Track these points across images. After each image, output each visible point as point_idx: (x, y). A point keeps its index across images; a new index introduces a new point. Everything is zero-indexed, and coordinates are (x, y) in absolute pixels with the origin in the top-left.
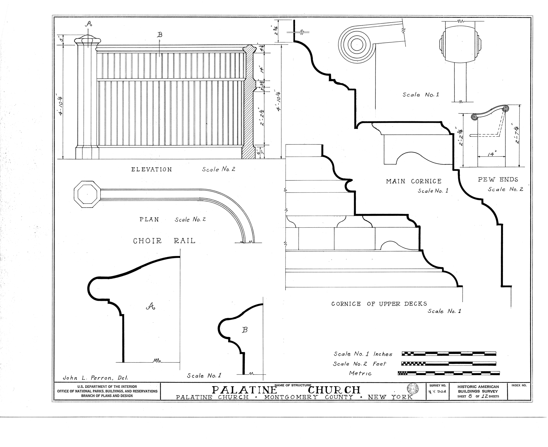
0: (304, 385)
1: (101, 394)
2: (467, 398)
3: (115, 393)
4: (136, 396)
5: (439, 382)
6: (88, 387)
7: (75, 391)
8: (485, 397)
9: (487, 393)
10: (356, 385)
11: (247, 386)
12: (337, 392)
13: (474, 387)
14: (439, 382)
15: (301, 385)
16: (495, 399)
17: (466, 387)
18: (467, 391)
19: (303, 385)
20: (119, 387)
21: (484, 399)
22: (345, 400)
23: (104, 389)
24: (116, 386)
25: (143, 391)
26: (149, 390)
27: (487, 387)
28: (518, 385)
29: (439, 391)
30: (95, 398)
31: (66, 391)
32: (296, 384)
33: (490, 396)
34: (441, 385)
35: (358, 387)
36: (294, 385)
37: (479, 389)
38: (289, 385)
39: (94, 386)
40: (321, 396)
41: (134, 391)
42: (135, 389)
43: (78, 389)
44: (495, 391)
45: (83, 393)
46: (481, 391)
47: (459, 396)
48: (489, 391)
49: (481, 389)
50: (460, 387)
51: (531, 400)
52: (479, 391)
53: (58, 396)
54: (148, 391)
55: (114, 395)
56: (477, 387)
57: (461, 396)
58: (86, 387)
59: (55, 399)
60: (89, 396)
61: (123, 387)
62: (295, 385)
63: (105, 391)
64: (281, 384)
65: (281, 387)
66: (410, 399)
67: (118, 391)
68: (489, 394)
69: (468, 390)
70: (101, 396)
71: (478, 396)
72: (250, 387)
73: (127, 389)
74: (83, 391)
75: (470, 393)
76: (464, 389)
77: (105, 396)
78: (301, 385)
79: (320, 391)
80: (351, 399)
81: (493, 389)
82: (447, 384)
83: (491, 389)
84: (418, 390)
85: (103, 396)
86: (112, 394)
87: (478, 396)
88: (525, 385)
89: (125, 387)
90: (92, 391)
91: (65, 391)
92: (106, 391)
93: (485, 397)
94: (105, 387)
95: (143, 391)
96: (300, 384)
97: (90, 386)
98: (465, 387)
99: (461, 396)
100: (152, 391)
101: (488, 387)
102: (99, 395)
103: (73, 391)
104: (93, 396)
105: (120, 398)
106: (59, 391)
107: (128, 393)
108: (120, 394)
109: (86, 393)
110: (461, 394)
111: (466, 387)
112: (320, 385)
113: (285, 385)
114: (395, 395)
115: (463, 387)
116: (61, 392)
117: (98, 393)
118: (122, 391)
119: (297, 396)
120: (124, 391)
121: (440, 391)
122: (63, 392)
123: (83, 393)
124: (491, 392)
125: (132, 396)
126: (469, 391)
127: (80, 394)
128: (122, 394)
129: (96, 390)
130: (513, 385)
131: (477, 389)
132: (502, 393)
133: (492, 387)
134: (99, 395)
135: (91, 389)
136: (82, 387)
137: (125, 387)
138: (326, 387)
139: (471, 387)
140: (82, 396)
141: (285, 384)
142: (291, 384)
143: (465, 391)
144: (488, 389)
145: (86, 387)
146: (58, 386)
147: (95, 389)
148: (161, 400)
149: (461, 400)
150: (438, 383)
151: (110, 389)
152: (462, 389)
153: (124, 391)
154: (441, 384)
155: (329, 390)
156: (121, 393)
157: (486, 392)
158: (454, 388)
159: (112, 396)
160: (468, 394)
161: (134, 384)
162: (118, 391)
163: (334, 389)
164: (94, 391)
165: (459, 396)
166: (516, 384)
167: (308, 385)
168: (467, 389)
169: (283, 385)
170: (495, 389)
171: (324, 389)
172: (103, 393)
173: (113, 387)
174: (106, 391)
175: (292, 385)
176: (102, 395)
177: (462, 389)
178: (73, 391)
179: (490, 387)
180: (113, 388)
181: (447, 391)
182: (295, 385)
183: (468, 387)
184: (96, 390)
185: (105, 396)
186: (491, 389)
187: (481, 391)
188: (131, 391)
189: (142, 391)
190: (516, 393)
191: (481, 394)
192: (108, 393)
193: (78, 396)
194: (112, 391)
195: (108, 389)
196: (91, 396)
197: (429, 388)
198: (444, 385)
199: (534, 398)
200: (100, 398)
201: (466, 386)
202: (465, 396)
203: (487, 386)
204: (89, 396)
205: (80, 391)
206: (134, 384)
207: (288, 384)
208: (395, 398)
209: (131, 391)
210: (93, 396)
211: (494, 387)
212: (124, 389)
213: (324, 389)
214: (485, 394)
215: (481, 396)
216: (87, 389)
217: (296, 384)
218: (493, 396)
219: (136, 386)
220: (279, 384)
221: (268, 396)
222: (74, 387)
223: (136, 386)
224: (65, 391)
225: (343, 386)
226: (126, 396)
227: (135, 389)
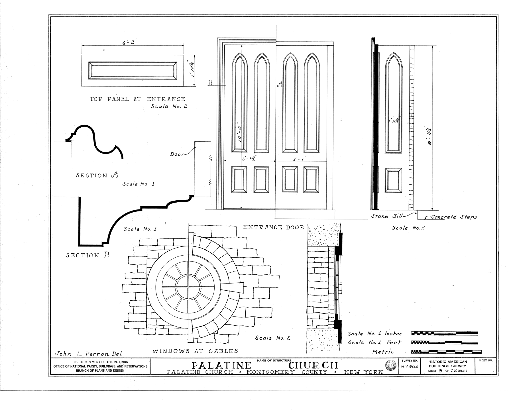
0: (285, 360)
1: (94, 368)
2: (437, 372)
3: (108, 368)
4: (127, 371)
5: (411, 358)
7: (70, 366)
8: (455, 371)
9: (456, 368)
10: (334, 361)
11: (222, 361)
12: (315, 367)
13: (444, 362)
14: (411, 358)
15: (282, 361)
16: (463, 373)
17: (437, 362)
18: (437, 366)
19: (283, 360)
20: (111, 362)
21: (454, 373)
23: (98, 364)
24: (108, 362)
25: (134, 366)
26: (139, 365)
27: (456, 362)
28: (485, 360)
29: (411, 366)
30: (89, 373)
31: (62, 366)
32: (277, 359)
33: (459, 371)
34: (413, 361)
35: (336, 363)
36: (275, 360)
37: (449, 364)
38: (270, 360)
39: (89, 362)
40: (298, 371)
41: (125, 366)
42: (126, 364)
43: (73, 364)
44: (464, 366)
45: (78, 368)
46: (450, 366)
47: (429, 371)
48: (457, 366)
49: (450, 364)
50: (431, 362)
51: (497, 374)
52: (448, 366)
53: (54, 371)
54: (138, 366)
56: (447, 362)
57: (432, 371)
59: (51, 374)
60: (84, 371)
61: (115, 362)
62: (276, 360)
63: (98, 366)
64: (263, 359)
65: (263, 362)
66: (376, 374)
67: (110, 366)
68: (458, 368)
69: (438, 365)
70: (94, 370)
71: (448, 371)
72: (225, 362)
73: (119, 364)
75: (440, 368)
76: (435, 364)
78: (282, 361)
79: (299, 367)
81: (462, 364)
82: (419, 360)
83: (460, 364)
84: (396, 366)
85: (96, 371)
86: (105, 369)
87: (448, 371)
88: (491, 360)
89: (117, 362)
90: (86, 366)
91: (60, 366)
92: (100, 366)
93: (455, 371)
95: (134, 366)
96: (281, 359)
97: (84, 362)
98: (435, 362)
99: (432, 371)
100: (79, 366)
101: (457, 362)
102: (93, 370)
104: (88, 371)
105: (112, 373)
106: (55, 366)
107: (120, 368)
108: (112, 369)
109: (80, 368)
110: (431, 369)
111: (437, 362)
112: (299, 360)
113: (267, 360)
114: (367, 371)
115: (434, 362)
116: (57, 367)
117: (92, 368)
119: (276, 371)
120: (116, 366)
121: (412, 366)
122: (59, 367)
123: (78, 368)
124: (460, 367)
125: (123, 370)
126: (439, 366)
127: (75, 369)
128: (115, 368)
129: (90, 365)
130: (480, 360)
131: (447, 364)
132: (469, 367)
133: (461, 362)
134: (93, 370)
135: (86, 365)
136: (77, 362)
137: (117, 362)
138: (305, 363)
139: (441, 362)
140: (77, 371)
141: (267, 359)
142: (272, 359)
143: (435, 366)
144: (457, 364)
146: (54, 362)
147: (89, 364)
149: (431, 374)
150: (410, 358)
151: (103, 364)
152: (432, 364)
153: (116, 366)
154: (413, 359)
155: (307, 365)
156: (114, 368)
157: (455, 366)
158: (425, 363)
159: (105, 370)
160: (438, 369)
161: (126, 360)
162: (110, 366)
163: (312, 364)
164: (88, 366)
165: (429, 371)
166: (483, 359)
167: (288, 360)
168: (437, 364)
169: (265, 361)
170: (463, 364)
171: (303, 364)
172: (96, 368)
173: (106, 362)
174: (100, 366)
175: (274, 361)
176: (96, 370)
177: (432, 364)
179: (442, 362)
180: (106, 364)
181: (419, 366)
182: (276, 360)
183: (439, 362)
184: (90, 365)
185: (98, 371)
186: (460, 364)
187: (450, 366)
188: (122, 367)
189: (133, 366)
190: (483, 367)
191: (450, 368)
192: (101, 368)
193: (73, 371)
194: (105, 366)
195: (101, 364)
196: (86, 371)
197: (402, 363)
198: (416, 361)
199: (499, 373)
200: (94, 372)
201: (436, 361)
202: (435, 371)
203: (456, 361)
204: (84, 371)
205: (75, 366)
206: (126, 360)
207: (270, 359)
208: (368, 373)
209: (122, 367)
210: (88, 371)
211: (462, 362)
212: (116, 365)
213: (303, 364)
214: (454, 368)
215: (450, 370)
216: (82, 364)
217: (277, 359)
218: (461, 371)
219: (127, 362)
220: (261, 359)
221: (251, 371)
222: (69, 362)
223: (127, 362)
224: (60, 366)
225: (321, 361)
226: (118, 371)
227: (126, 364)
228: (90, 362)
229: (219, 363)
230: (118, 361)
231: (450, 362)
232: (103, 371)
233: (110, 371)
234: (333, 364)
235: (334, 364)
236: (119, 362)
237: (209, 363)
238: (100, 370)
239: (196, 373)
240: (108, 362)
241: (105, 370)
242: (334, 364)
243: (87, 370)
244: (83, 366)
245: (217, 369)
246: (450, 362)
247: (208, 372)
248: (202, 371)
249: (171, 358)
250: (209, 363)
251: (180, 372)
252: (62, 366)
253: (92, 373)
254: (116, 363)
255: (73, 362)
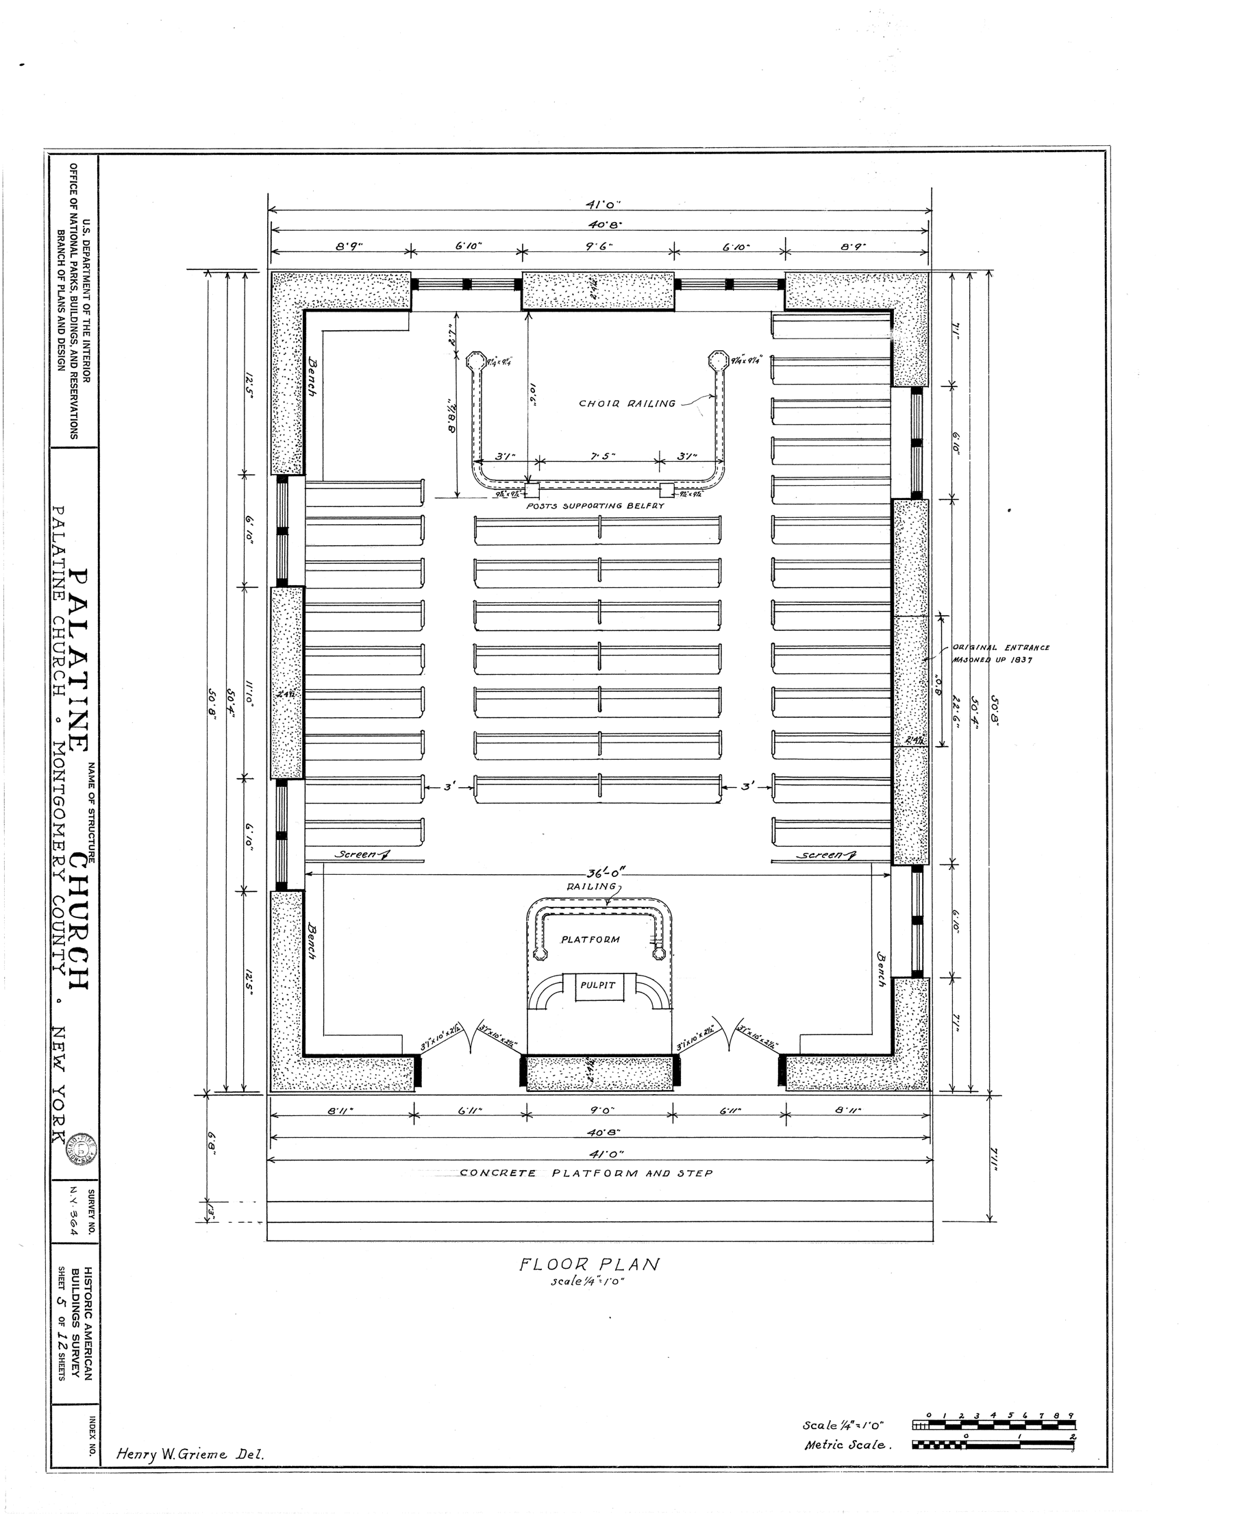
1: (67, 283)
4: (61, 381)
6: (86, 245)
7: (74, 211)
11: (90, 665)
20: (87, 332)
22: (50, 777)
23: (79, 293)
24: (87, 323)
25: (73, 401)
26: (76, 415)
30: (55, 268)
39: (87, 266)
41: (75, 374)
42: (80, 377)
43: (80, 220)
45: (67, 235)
53: (61, 166)
54: (74, 413)
55: (64, 319)
58: (84, 241)
60: (61, 252)
61: (87, 345)
63: (75, 293)
67: (74, 330)
70: (62, 283)
72: (86, 673)
73: (80, 356)
74: (74, 234)
77: (61, 294)
80: (54, 875)
85: (59, 289)
86: (66, 315)
89: (87, 350)
90: (75, 258)
91: (74, 183)
92: (74, 299)
94: (87, 295)
95: (73, 401)
97: (88, 254)
102: (62, 277)
103: (74, 206)
104: (61, 263)
105: (55, 335)
106: (74, 169)
107: (68, 358)
108: (67, 336)
109: (67, 242)
116: (72, 174)
117: (68, 276)
118: (74, 342)
120: (75, 347)
122: (72, 179)
123: (67, 235)
125: (62, 368)
128: (67, 343)
129: (76, 269)
134: (62, 277)
135: (79, 257)
136: (86, 231)
137: (87, 350)
140: (61, 232)
145: (84, 241)
146: (87, 166)
147: (80, 266)
148: (50, 448)
151: (80, 309)
153: (75, 347)
156: (68, 339)
159: (62, 315)
161: (94, 376)
162: (74, 330)
164: (75, 263)
172: (68, 288)
173: (86, 317)
174: (74, 299)
176: (63, 287)
178: (74, 206)
180: (82, 316)
184: (76, 269)
185: (62, 294)
189: (75, 397)
192: (68, 302)
193: (61, 221)
194: (74, 315)
195: (81, 302)
196: (61, 257)
200: (56, 281)
204: (61, 252)
205: (74, 225)
206: (94, 376)
210: (61, 263)
212: (79, 347)
216: (80, 246)
219: (87, 380)
222: (86, 210)
223: (87, 380)
224: (74, 183)
227: (80, 377)
228: (87, 270)
229: (85, 657)
230: (89, 352)
231: (91, 775)
232: (61, 308)
233: (61, 329)
234: (83, 883)
235: (84, 886)
236: (87, 354)
237: (85, 625)
238: (64, 298)
239: (56, 590)
240: (87, 323)
241: (62, 315)
242: (84, 886)
243: (61, 261)
244: (74, 251)
245: (67, 651)
246: (91, 775)
247: (58, 624)
248: (61, 607)
249: (99, 228)
250: (85, 625)
251: (59, 542)
252: (74, 187)
253: (54, 275)
254: (84, 348)
255: (85, 222)
